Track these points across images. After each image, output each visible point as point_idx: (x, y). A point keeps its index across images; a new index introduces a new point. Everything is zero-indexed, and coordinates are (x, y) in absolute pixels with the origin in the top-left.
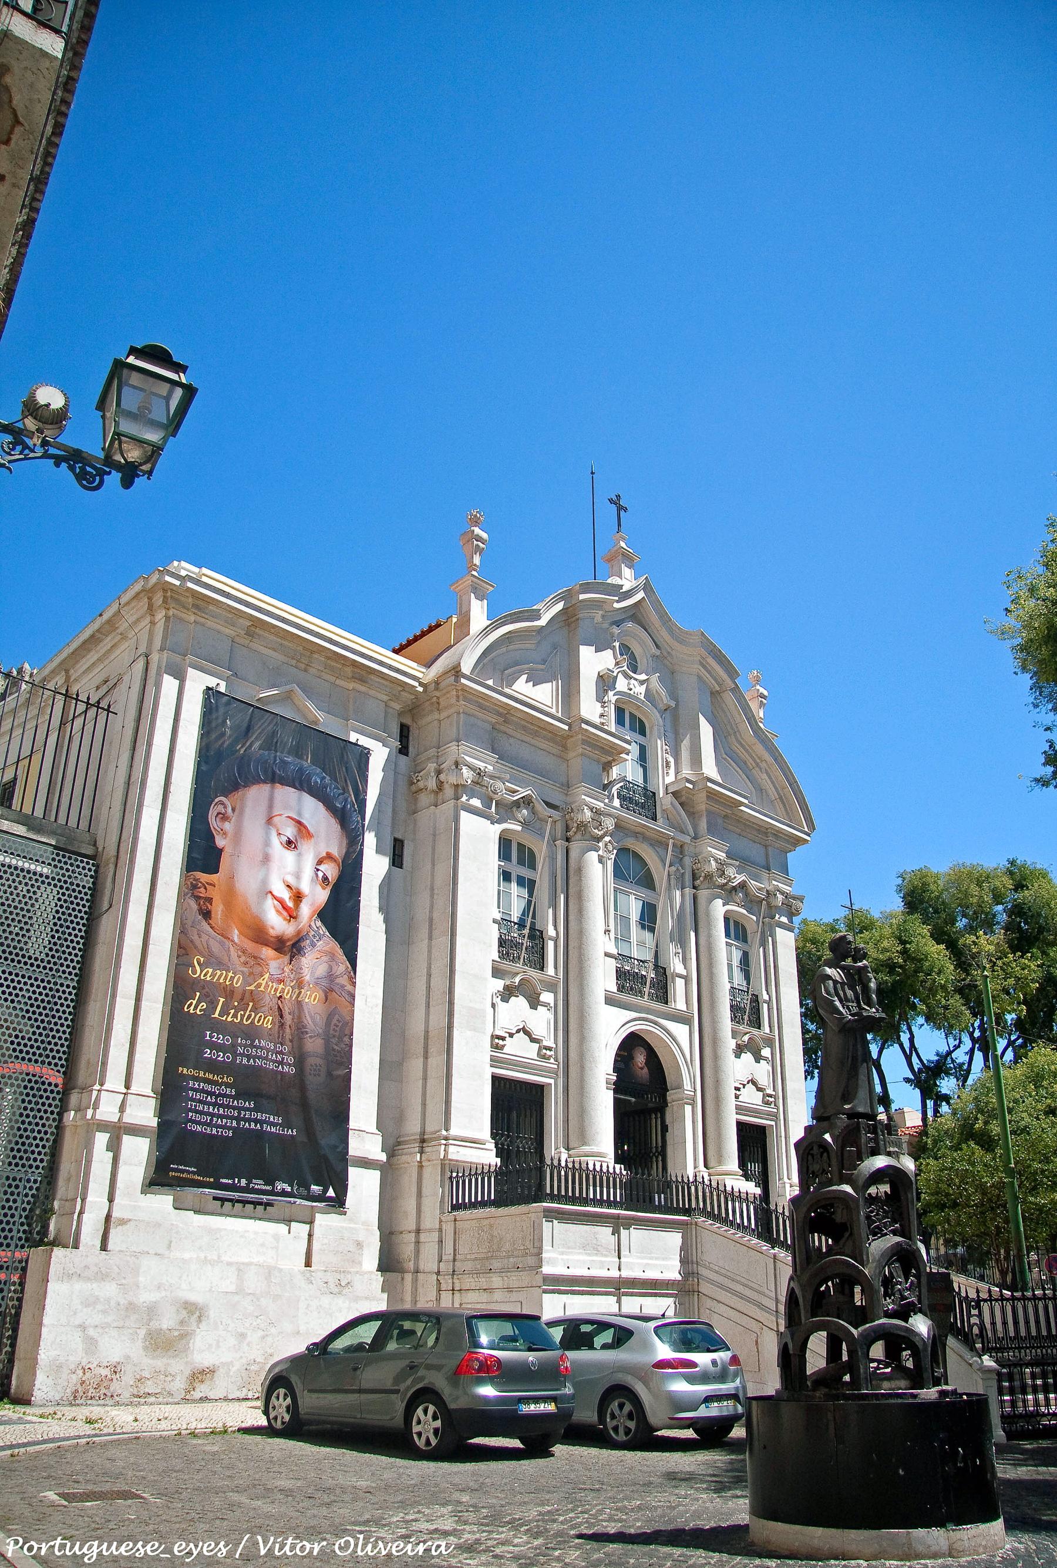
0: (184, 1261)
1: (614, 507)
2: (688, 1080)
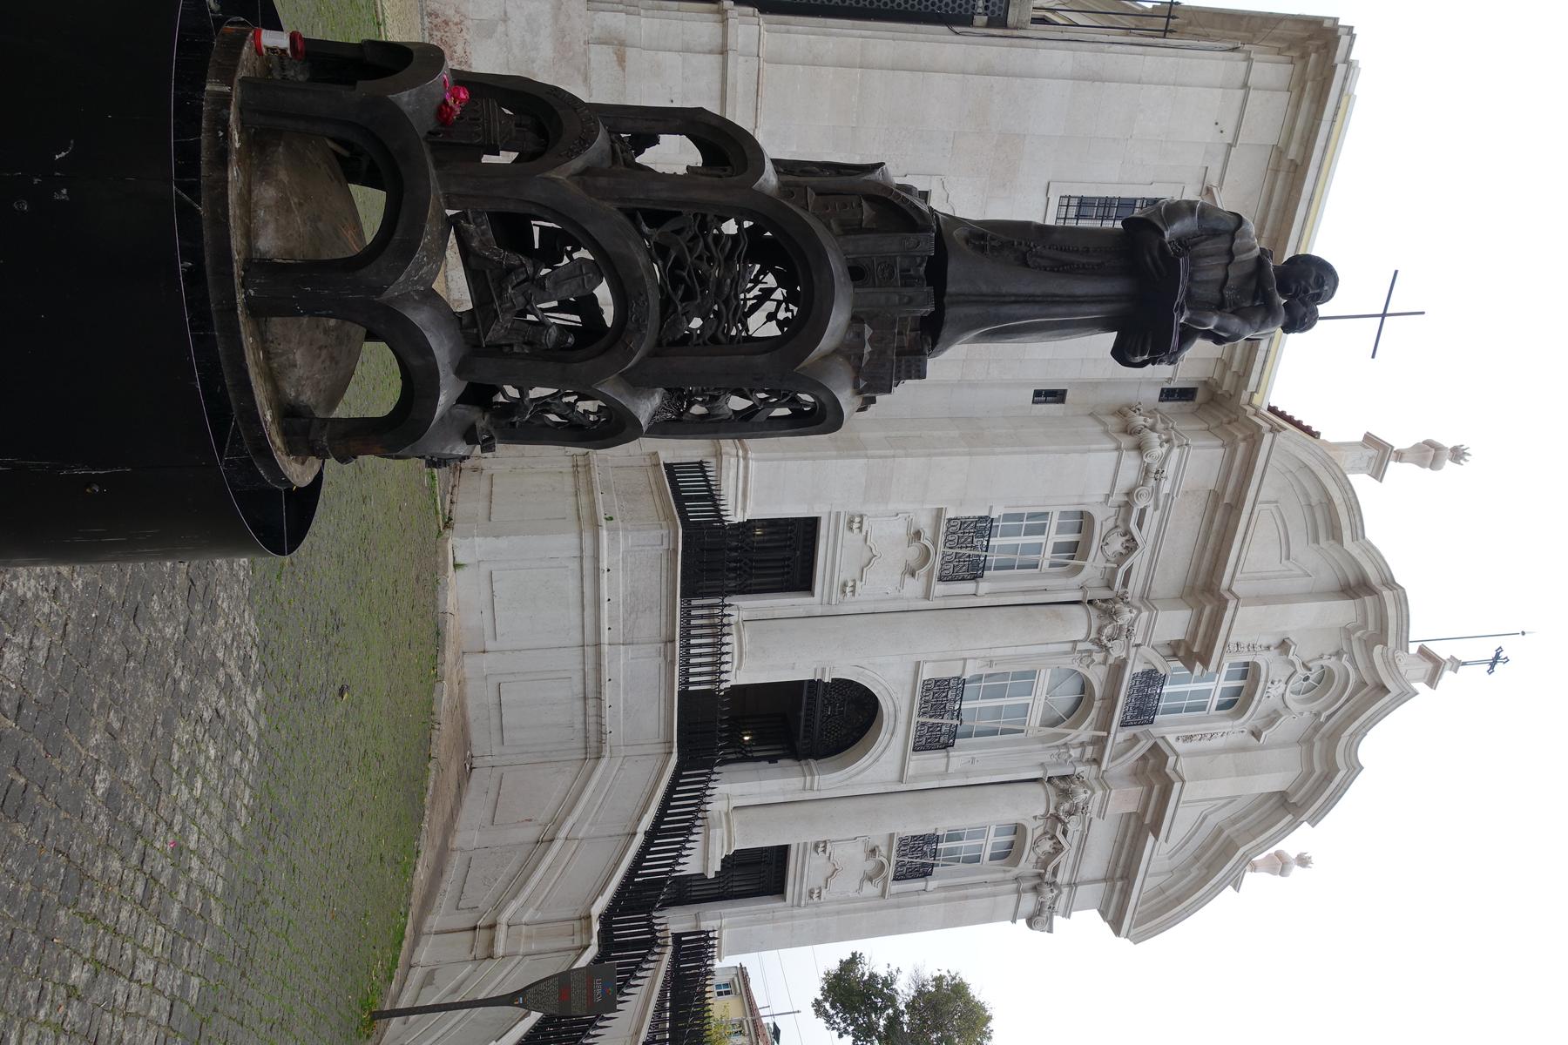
2: (830, 780)
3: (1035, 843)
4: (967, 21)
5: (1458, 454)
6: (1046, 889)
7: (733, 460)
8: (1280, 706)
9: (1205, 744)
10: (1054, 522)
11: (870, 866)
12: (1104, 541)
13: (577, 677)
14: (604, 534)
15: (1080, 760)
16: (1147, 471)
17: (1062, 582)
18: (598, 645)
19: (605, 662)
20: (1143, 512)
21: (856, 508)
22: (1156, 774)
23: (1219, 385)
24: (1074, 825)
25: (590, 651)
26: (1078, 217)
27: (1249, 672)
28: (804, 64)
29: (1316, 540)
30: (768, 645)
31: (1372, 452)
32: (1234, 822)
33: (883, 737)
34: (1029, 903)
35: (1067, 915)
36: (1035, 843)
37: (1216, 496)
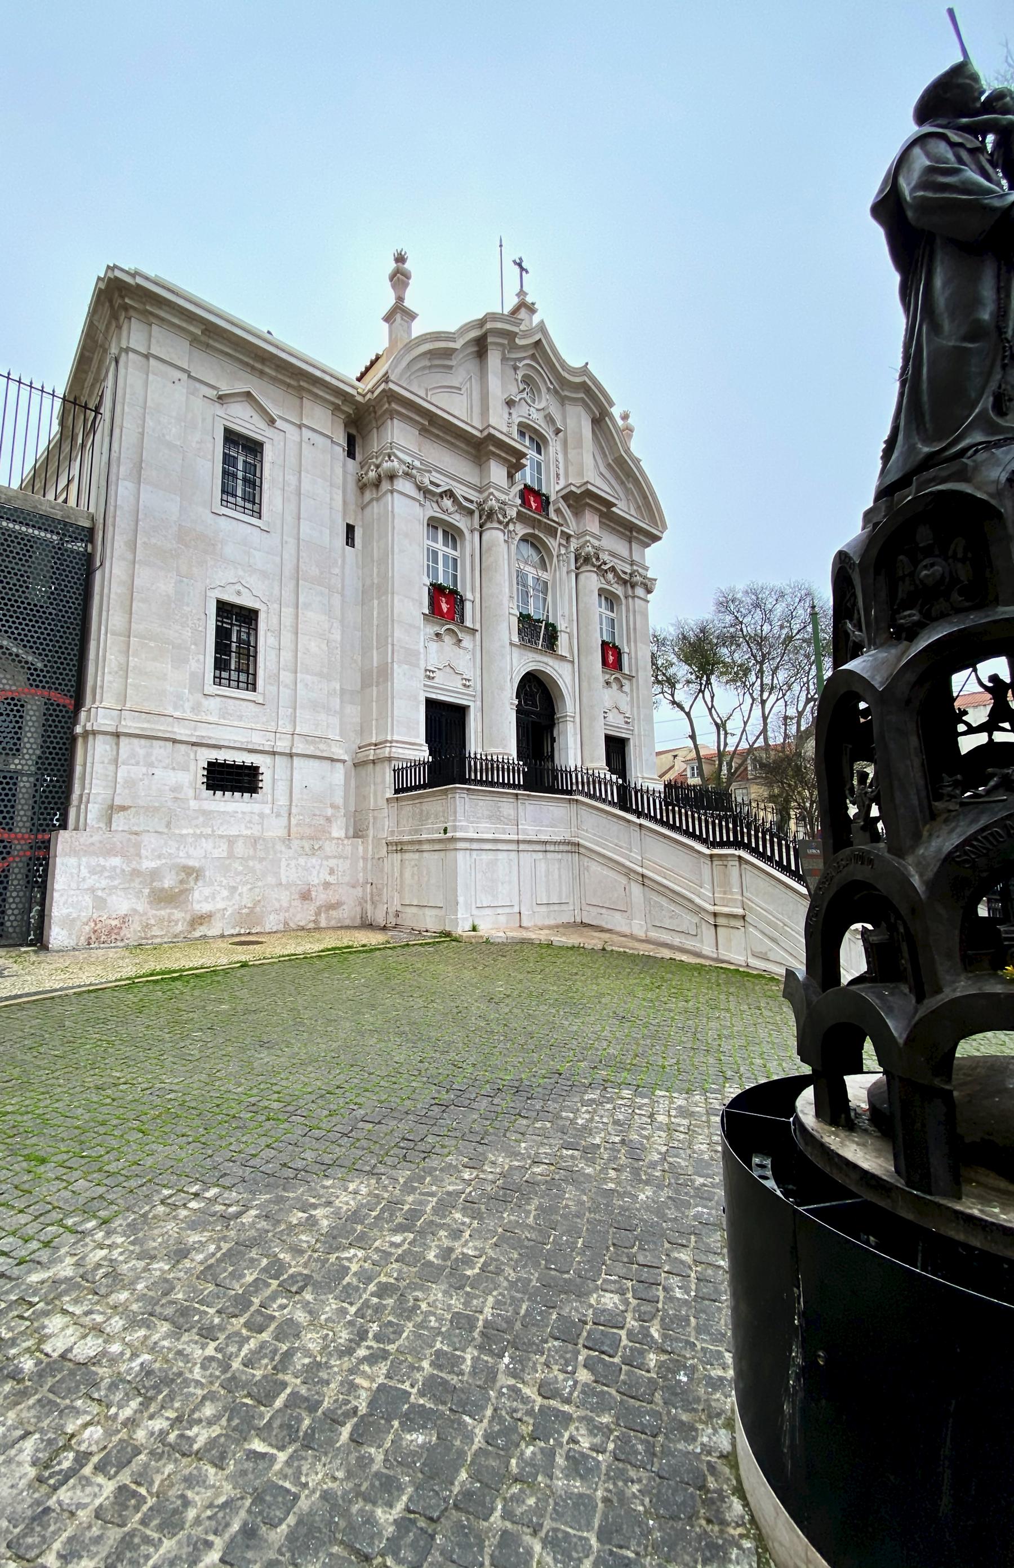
0: (182, 835)
1: (517, 269)
2: (570, 706)
3: (608, 583)
4: (89, 558)
5: (400, 259)
6: (635, 579)
7: (394, 750)
8: (542, 414)
9: (561, 466)
10: (430, 543)
11: (615, 686)
12: (445, 511)
13: (535, 855)
14: (458, 835)
15: (566, 548)
16: (407, 474)
17: (468, 544)
18: (518, 842)
19: (528, 838)
20: (431, 482)
21: (421, 674)
22: (580, 500)
23: (349, 415)
24: (605, 557)
25: (522, 847)
26: (235, 496)
27: (524, 429)
28: (127, 678)
29: (450, 367)
30: (494, 735)
31: (398, 316)
32: (605, 455)
33: (548, 670)
34: (640, 591)
35: (646, 569)
36: (608, 583)
37: (423, 431)
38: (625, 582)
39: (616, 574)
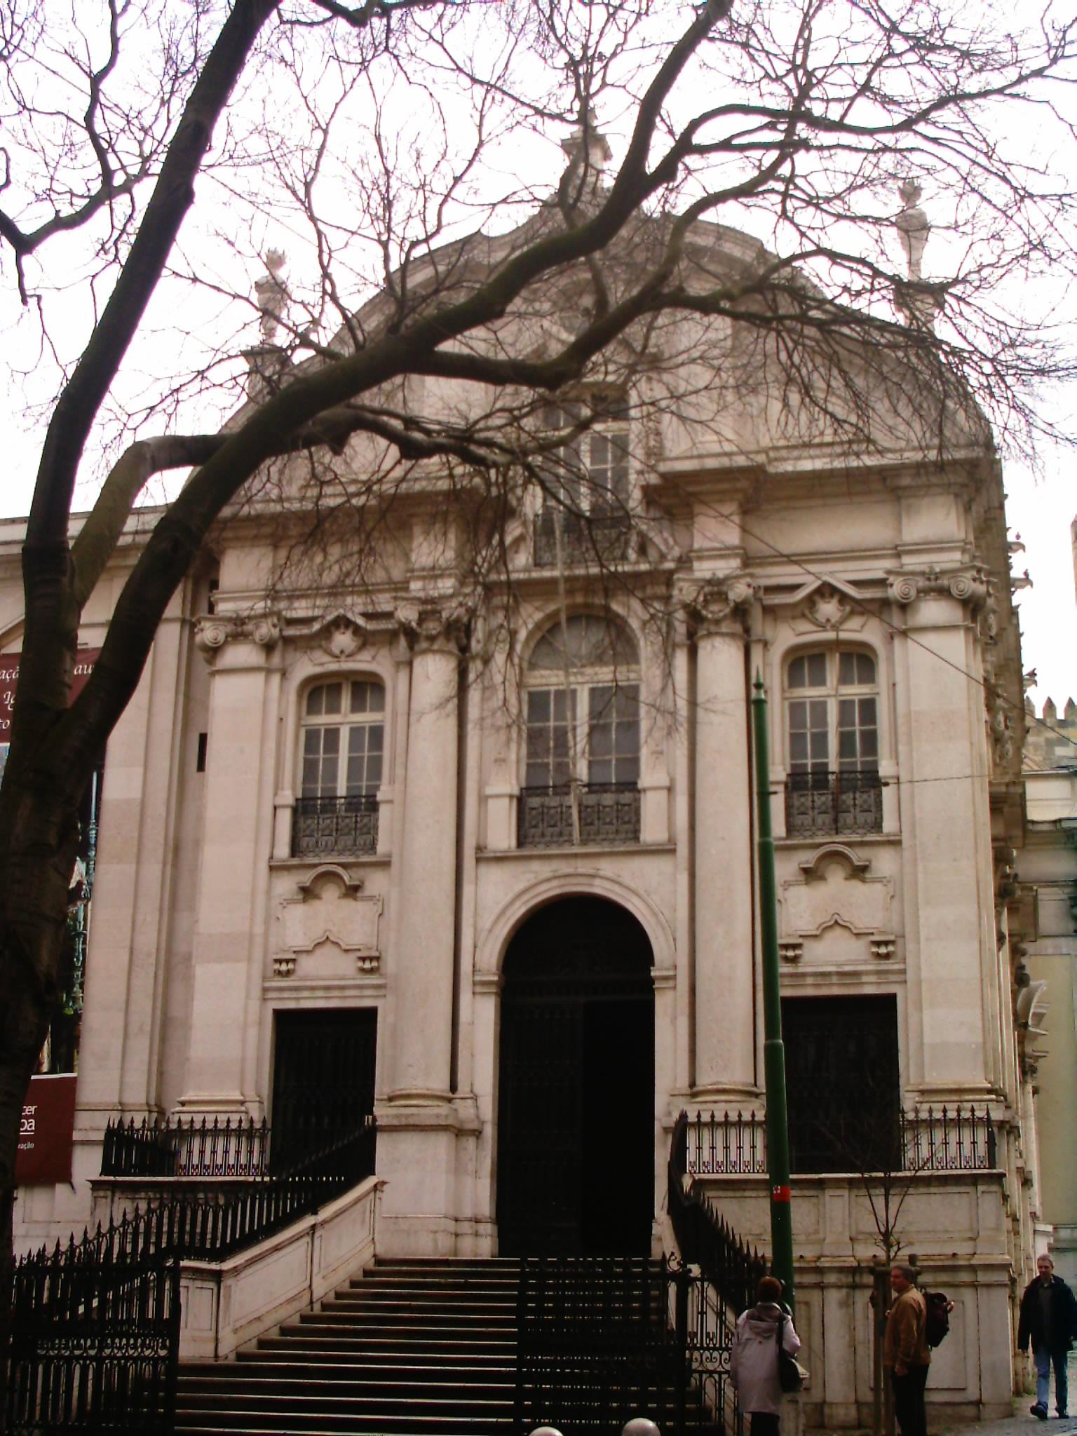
24: (740, 591)
38: (882, 607)
39: (844, 598)
